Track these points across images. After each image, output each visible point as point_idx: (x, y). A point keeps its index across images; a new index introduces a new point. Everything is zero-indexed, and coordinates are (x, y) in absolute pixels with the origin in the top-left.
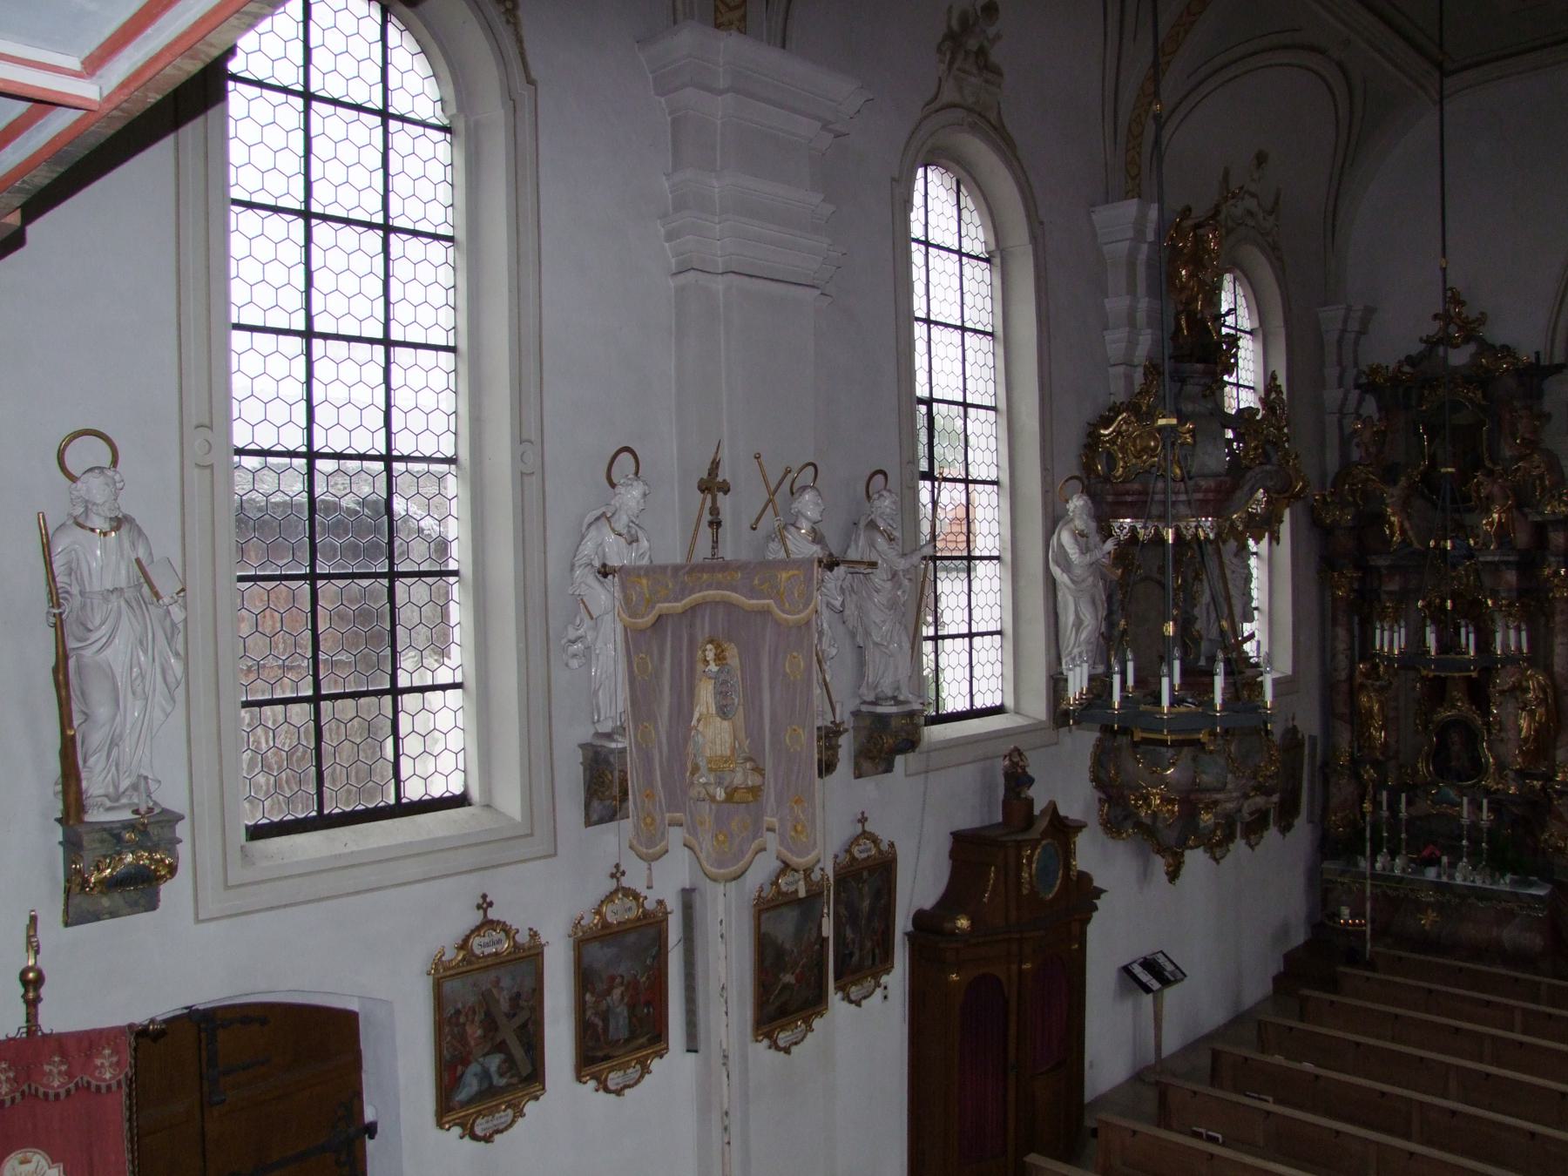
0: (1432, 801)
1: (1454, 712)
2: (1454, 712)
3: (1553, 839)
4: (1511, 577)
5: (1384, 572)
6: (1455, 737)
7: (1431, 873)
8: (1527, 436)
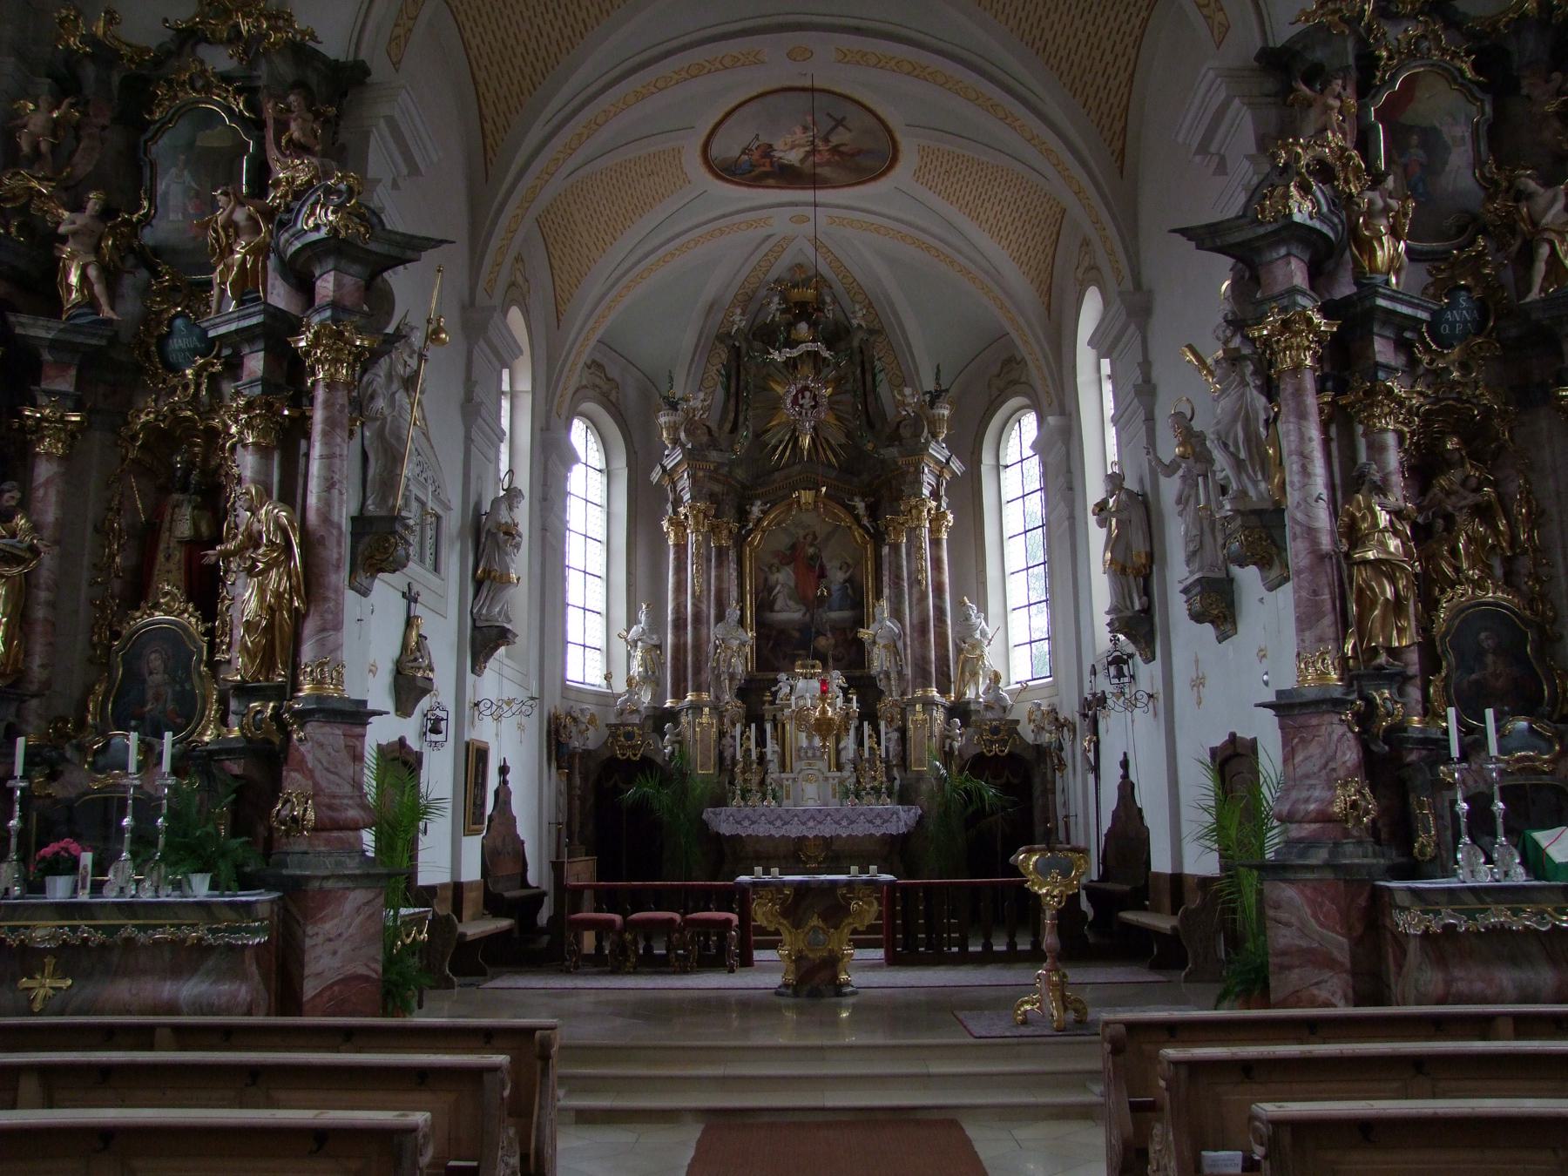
0: (93, 765)
1: (159, 616)
2: (159, 616)
3: (288, 805)
4: (255, 363)
5: (47, 356)
6: (155, 660)
7: (59, 889)
8: (296, 135)
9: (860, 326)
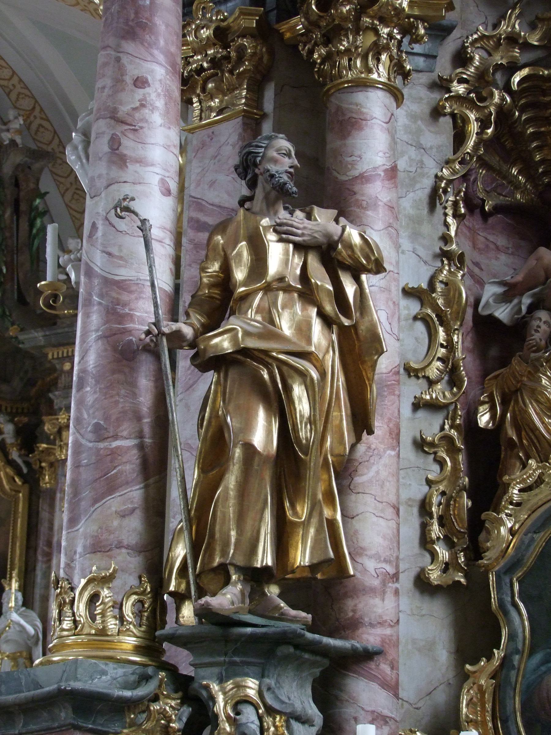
9: (13, 142)
